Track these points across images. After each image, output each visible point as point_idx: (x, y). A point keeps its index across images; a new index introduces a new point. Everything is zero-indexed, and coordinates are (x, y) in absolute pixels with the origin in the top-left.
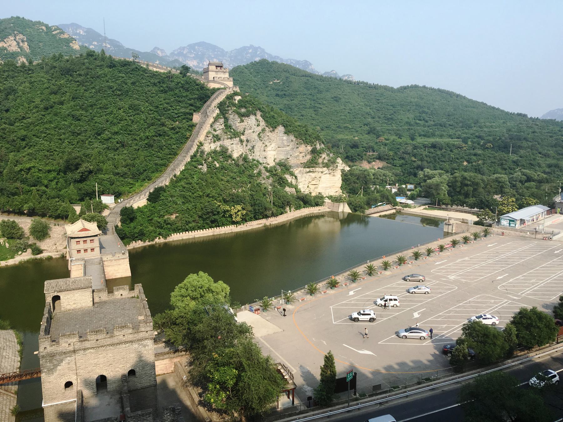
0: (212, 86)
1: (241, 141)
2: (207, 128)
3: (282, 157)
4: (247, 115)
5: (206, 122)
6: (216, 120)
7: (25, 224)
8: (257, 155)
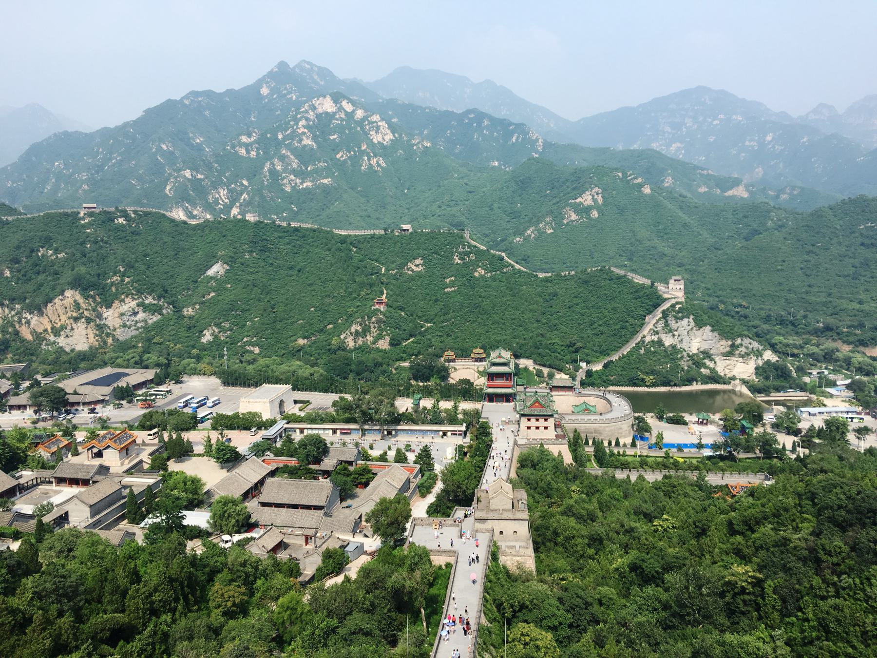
0: (666, 296)
1: (674, 335)
2: (651, 326)
3: (705, 346)
4: (682, 318)
5: (652, 321)
6: (658, 321)
7: (546, 371)
8: (684, 345)
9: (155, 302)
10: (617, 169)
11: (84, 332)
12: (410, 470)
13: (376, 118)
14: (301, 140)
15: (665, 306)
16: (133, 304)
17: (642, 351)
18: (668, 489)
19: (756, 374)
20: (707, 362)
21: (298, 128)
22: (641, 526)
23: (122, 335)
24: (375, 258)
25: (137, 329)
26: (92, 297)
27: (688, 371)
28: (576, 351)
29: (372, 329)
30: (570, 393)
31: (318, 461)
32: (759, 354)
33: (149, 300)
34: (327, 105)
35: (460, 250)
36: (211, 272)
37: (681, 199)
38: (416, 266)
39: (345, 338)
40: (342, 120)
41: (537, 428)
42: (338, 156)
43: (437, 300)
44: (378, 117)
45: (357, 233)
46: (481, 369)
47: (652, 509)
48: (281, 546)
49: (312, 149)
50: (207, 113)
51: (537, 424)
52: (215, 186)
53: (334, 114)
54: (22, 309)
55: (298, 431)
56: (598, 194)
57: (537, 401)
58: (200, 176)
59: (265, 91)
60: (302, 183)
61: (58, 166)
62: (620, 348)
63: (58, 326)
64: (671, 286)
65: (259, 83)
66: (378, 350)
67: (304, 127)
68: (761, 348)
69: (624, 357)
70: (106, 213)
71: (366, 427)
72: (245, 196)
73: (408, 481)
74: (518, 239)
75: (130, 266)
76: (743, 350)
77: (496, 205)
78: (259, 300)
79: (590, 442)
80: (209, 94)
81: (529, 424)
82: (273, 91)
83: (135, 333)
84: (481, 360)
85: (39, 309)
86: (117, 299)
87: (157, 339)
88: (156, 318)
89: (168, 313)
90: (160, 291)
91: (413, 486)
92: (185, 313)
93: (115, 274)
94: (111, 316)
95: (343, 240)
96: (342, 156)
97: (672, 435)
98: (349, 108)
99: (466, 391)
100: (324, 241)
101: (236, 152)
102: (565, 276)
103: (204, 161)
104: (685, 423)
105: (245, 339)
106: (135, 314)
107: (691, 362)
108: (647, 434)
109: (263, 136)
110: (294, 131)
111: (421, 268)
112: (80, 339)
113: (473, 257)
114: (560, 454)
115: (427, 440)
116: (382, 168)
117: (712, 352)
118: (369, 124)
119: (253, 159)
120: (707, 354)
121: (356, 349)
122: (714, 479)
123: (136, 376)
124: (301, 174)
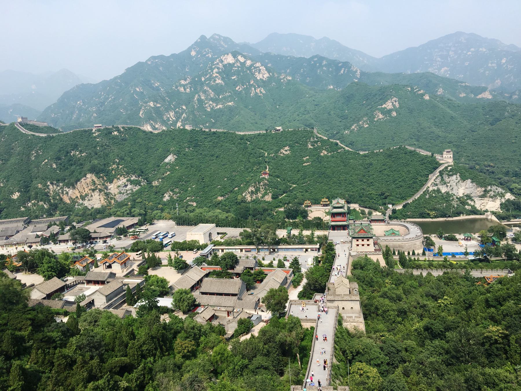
0: (441, 162)
1: (447, 186)
2: (432, 181)
3: (467, 192)
4: (452, 175)
5: (433, 178)
6: (437, 178)
7: (367, 211)
8: (454, 192)
9: (137, 179)
10: (407, 86)
11: (98, 197)
12: (287, 272)
13: (258, 64)
15: (441, 168)
16: (125, 180)
17: (427, 197)
18: (447, 280)
19: (501, 208)
20: (469, 202)
21: (213, 74)
22: (430, 304)
23: (120, 198)
24: (261, 147)
25: (128, 195)
26: (101, 177)
27: (457, 208)
28: (386, 198)
29: (261, 190)
30: (383, 224)
31: (233, 268)
32: (502, 195)
33: (133, 178)
34: (229, 59)
35: (312, 140)
36: (167, 160)
37: (449, 101)
38: (286, 151)
39: (245, 195)
40: (238, 67)
41: (363, 245)
42: (237, 89)
43: (299, 171)
45: (250, 133)
46: (327, 211)
47: (437, 293)
48: (214, 317)
49: (222, 85)
50: (161, 68)
51: (363, 243)
52: (167, 110)
53: (234, 64)
54: (63, 185)
55: (220, 250)
56: (395, 102)
57: (362, 229)
58: (158, 105)
59: (193, 53)
62: (413, 195)
63: (84, 194)
64: (444, 156)
65: (190, 49)
66: (265, 202)
67: (217, 73)
68: (503, 191)
69: (416, 200)
71: (260, 247)
72: (184, 115)
73: (286, 278)
74: (346, 132)
75: (122, 159)
76: (492, 193)
77: (332, 112)
78: (195, 175)
79: (397, 253)
80: (162, 57)
81: (358, 243)
82: (198, 53)
83: (126, 197)
84: (327, 205)
85: (73, 185)
86: (116, 178)
87: (139, 200)
88: (138, 188)
89: (144, 185)
90: (139, 172)
91: (289, 281)
92: (154, 184)
93: (114, 164)
94: (113, 188)
95: (242, 138)
96: (239, 89)
97: (448, 247)
98: (242, 60)
99: (319, 224)
100: (231, 138)
101: (178, 90)
102: (377, 153)
103: (160, 96)
104: (456, 240)
105: (188, 198)
106: (126, 186)
107: (459, 202)
108: (432, 247)
109: (193, 79)
111: (288, 152)
112: (96, 201)
113: (319, 144)
114: (378, 260)
115: (296, 254)
116: (263, 94)
117: (472, 195)
118: (254, 69)
119: (188, 93)
120: (469, 197)
121: (252, 201)
122: (475, 274)
123: (128, 222)
124: (216, 101)
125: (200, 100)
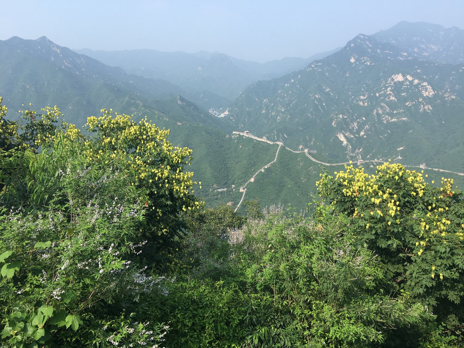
14: (390, 97)
21: (387, 91)
34: (399, 78)
40: (407, 85)
42: (407, 104)
44: (427, 83)
50: (327, 74)
53: (403, 81)
58: (345, 117)
59: (352, 60)
60: (391, 119)
61: (266, 101)
67: (390, 91)
70: (366, 163)
72: (367, 126)
82: (357, 60)
96: (409, 104)
98: (410, 78)
101: (358, 104)
110: (385, 93)
116: (430, 110)
119: (365, 107)
124: (392, 115)
125: (378, 114)
